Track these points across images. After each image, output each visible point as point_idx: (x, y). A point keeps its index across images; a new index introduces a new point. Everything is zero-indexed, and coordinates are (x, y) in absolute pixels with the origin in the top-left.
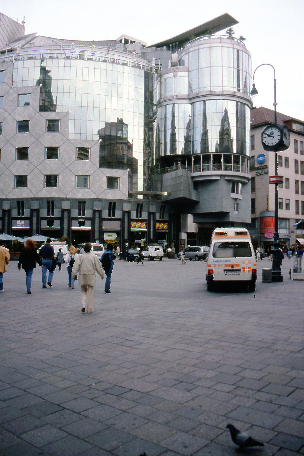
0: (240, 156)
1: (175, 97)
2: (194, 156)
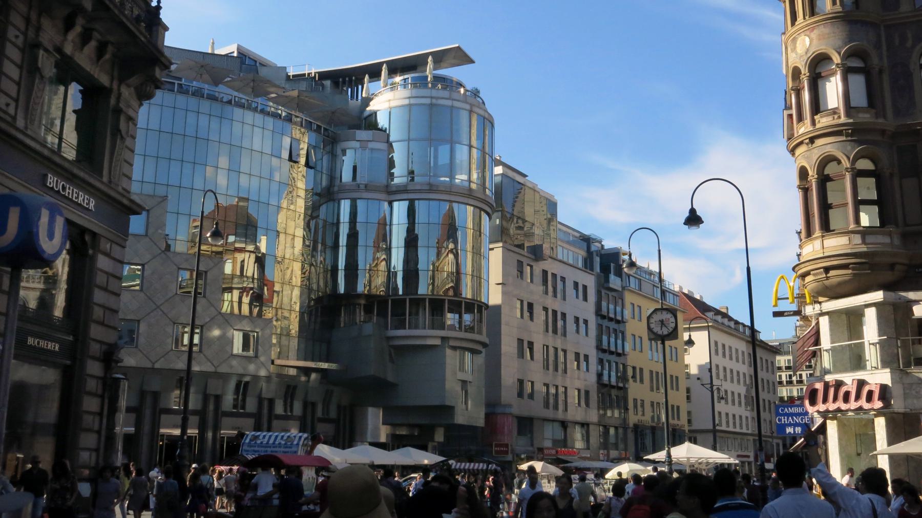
0: (474, 304)
1: (362, 187)
2: (392, 300)
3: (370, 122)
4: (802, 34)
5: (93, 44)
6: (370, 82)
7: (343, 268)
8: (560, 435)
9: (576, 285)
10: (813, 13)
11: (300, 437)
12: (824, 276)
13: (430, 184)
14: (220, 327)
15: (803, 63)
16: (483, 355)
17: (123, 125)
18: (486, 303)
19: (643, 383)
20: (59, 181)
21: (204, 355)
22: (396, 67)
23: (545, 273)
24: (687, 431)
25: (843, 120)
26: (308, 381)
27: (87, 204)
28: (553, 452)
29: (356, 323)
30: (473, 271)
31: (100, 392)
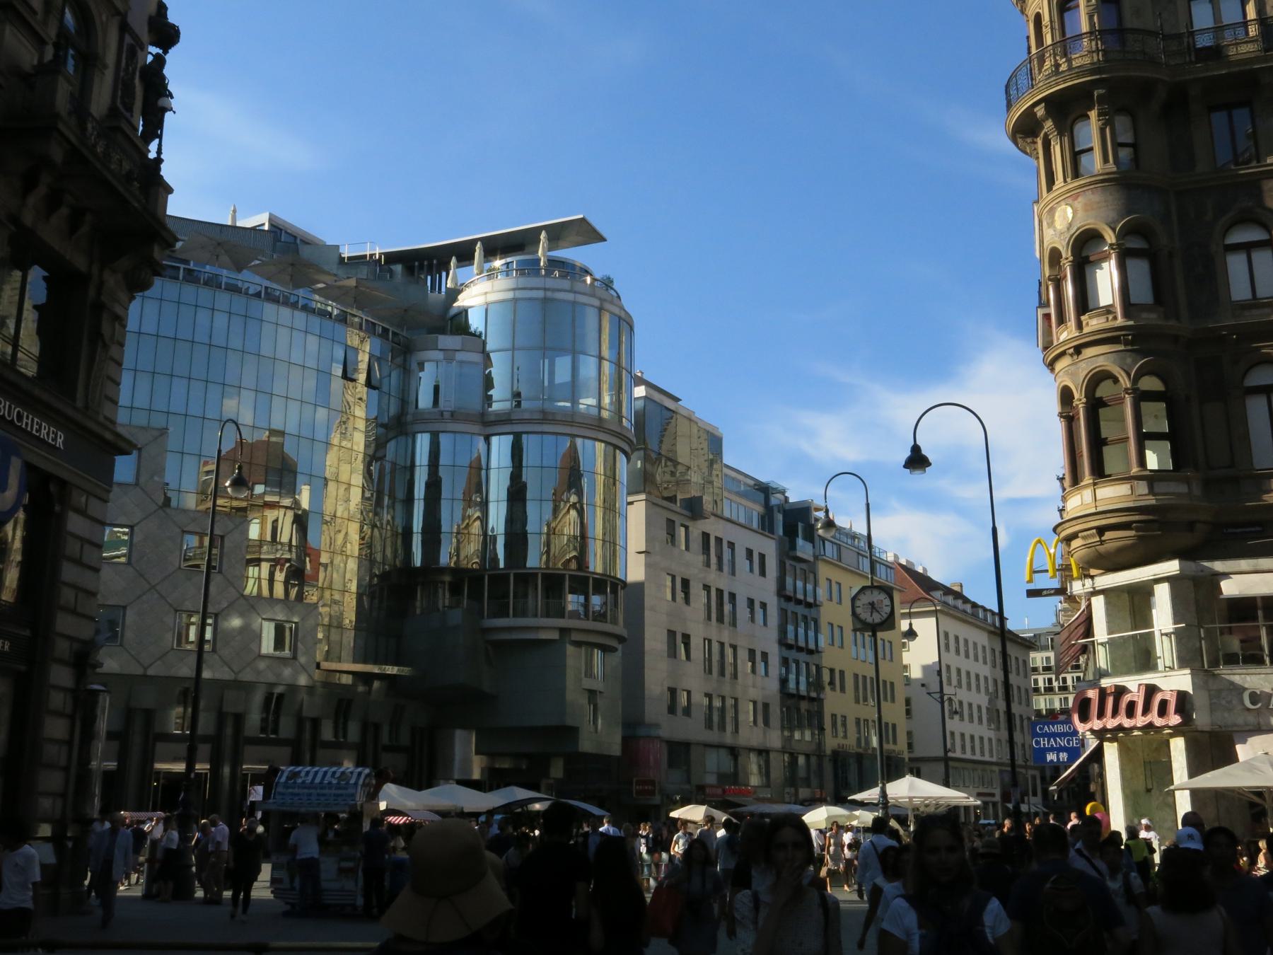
0: (605, 582)
1: (447, 415)
2: (489, 575)
3: (458, 324)
4: (1063, 203)
5: (64, 211)
6: (458, 267)
7: (420, 531)
8: (727, 764)
9: (750, 553)
10: (1076, 174)
11: (360, 774)
12: (1098, 539)
13: (543, 412)
14: (242, 615)
15: (1065, 243)
16: (619, 653)
17: (106, 328)
18: (623, 579)
19: (844, 692)
20: (13, 406)
21: (220, 657)
22: (496, 247)
23: (706, 536)
24: (907, 760)
25: (1120, 321)
26: (369, 692)
27: (53, 440)
28: (719, 791)
29: (438, 610)
30: (604, 534)
31: (69, 710)
